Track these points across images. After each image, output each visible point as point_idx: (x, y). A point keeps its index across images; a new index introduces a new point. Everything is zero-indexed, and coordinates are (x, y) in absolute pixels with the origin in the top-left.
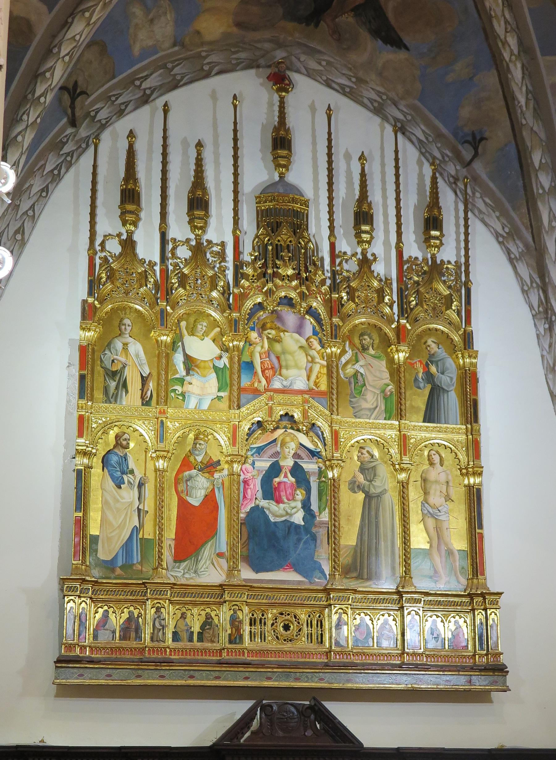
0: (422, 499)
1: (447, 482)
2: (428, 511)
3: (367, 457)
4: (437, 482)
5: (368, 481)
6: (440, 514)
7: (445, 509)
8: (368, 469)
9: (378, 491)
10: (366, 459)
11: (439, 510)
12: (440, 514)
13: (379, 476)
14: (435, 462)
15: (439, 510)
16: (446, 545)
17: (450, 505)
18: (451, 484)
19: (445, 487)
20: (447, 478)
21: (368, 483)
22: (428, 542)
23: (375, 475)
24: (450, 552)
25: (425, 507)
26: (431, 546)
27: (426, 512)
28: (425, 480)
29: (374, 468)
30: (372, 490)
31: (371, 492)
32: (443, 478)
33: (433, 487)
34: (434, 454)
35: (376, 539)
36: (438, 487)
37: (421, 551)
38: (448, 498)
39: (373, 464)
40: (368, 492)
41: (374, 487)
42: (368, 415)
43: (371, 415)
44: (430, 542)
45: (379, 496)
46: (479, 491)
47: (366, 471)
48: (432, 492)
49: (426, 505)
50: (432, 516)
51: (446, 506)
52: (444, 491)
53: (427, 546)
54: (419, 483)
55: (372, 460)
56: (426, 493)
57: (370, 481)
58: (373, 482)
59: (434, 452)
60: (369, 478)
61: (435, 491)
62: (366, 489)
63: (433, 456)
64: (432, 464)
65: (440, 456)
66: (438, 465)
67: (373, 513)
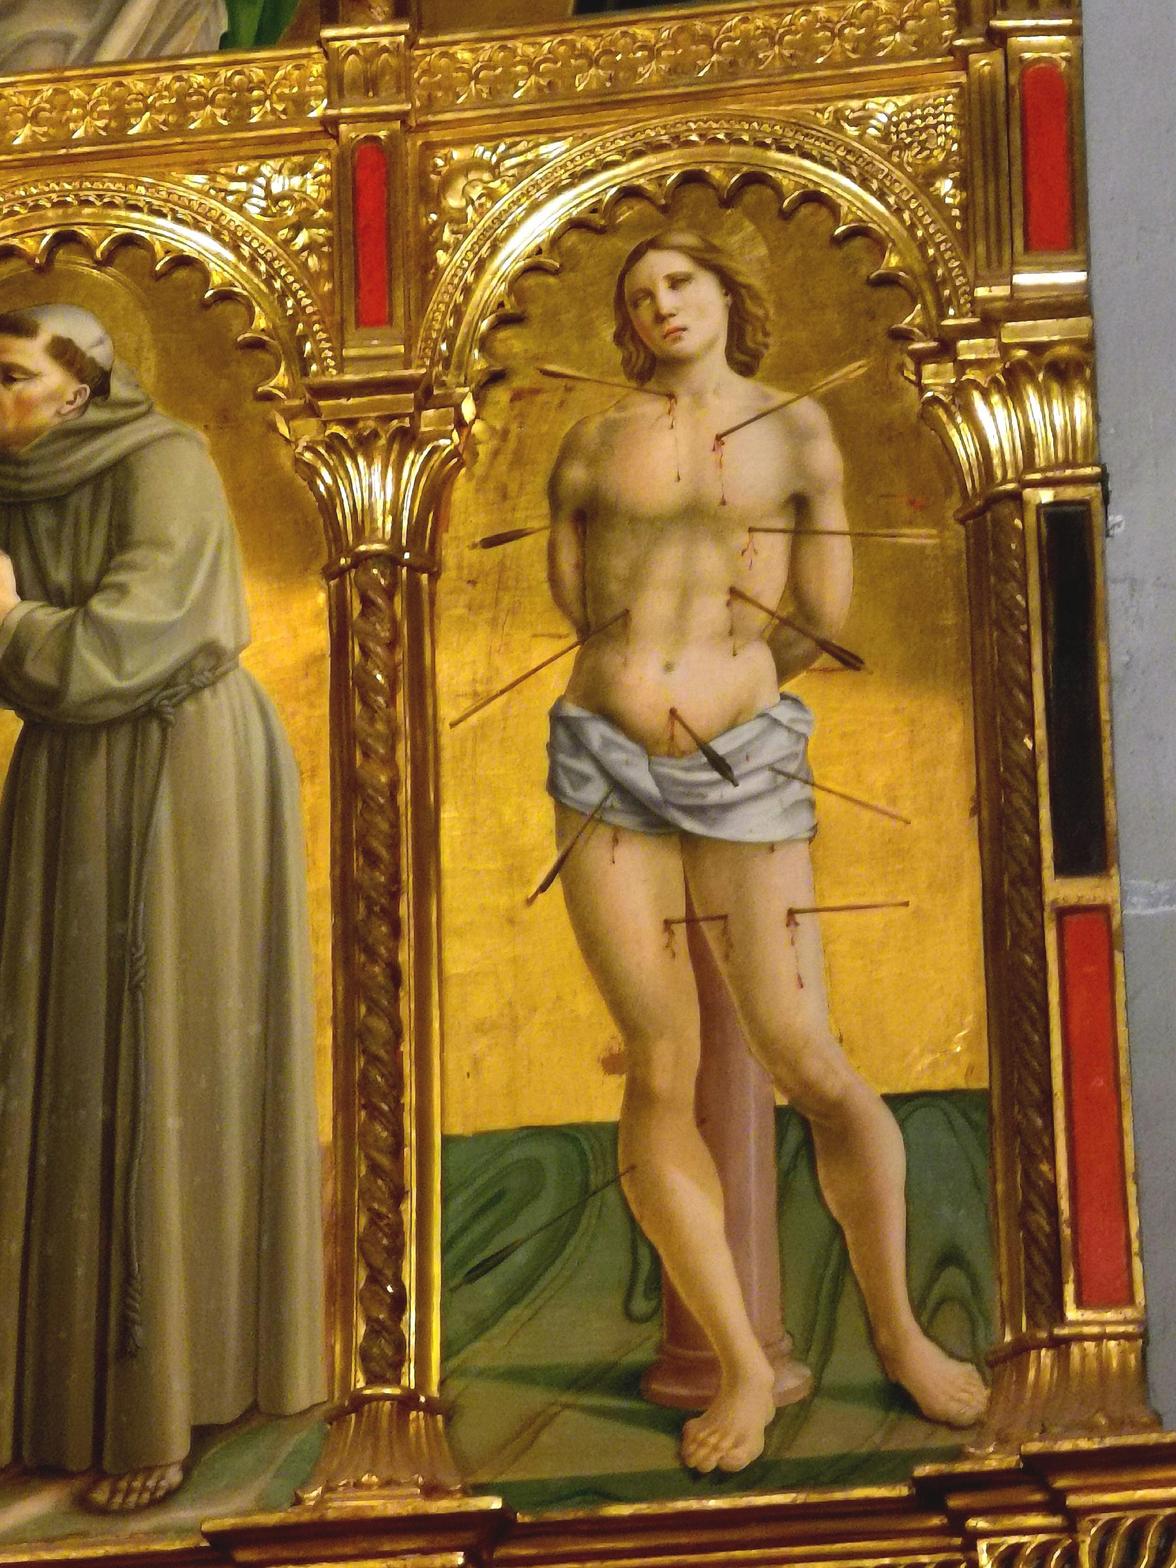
0: (555, 682)
1: (800, 506)
2: (618, 787)
3: (52, 397)
4: (698, 516)
5: (54, 597)
6: (729, 792)
7: (776, 746)
8: (57, 500)
9: (145, 668)
10: (45, 416)
11: (719, 764)
12: (729, 792)
13: (160, 544)
14: (688, 344)
15: (719, 764)
16: (778, 1055)
17: (826, 698)
18: (833, 513)
19: (772, 551)
20: (798, 465)
21: (48, 616)
22: (611, 1064)
23: (121, 538)
24: (811, 1131)
25: (579, 746)
26: (639, 1097)
27: (594, 792)
28: (588, 517)
29: (116, 483)
30: (94, 672)
31: (78, 688)
32: (755, 470)
33: (668, 562)
34: (676, 282)
35: (110, 1100)
36: (711, 561)
37: (533, 1149)
38: (799, 639)
39: (105, 450)
40: (53, 696)
41: (112, 642)
42: (67, 41)
43: (98, 40)
44: (630, 1062)
45: (152, 715)
46: (1071, 538)
47: (44, 520)
48: (654, 607)
49: (597, 732)
50: (653, 819)
51: (784, 713)
52: (768, 579)
53: (604, 1102)
54: (531, 549)
55: (95, 415)
56: (598, 623)
57: (77, 597)
58: (98, 605)
59: (662, 264)
60: (60, 575)
61: (686, 594)
62: (40, 671)
63: (667, 300)
64: (653, 365)
65: (729, 284)
66: (713, 367)
67: (93, 871)
